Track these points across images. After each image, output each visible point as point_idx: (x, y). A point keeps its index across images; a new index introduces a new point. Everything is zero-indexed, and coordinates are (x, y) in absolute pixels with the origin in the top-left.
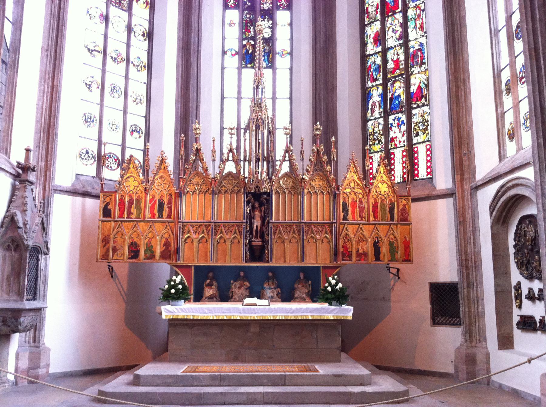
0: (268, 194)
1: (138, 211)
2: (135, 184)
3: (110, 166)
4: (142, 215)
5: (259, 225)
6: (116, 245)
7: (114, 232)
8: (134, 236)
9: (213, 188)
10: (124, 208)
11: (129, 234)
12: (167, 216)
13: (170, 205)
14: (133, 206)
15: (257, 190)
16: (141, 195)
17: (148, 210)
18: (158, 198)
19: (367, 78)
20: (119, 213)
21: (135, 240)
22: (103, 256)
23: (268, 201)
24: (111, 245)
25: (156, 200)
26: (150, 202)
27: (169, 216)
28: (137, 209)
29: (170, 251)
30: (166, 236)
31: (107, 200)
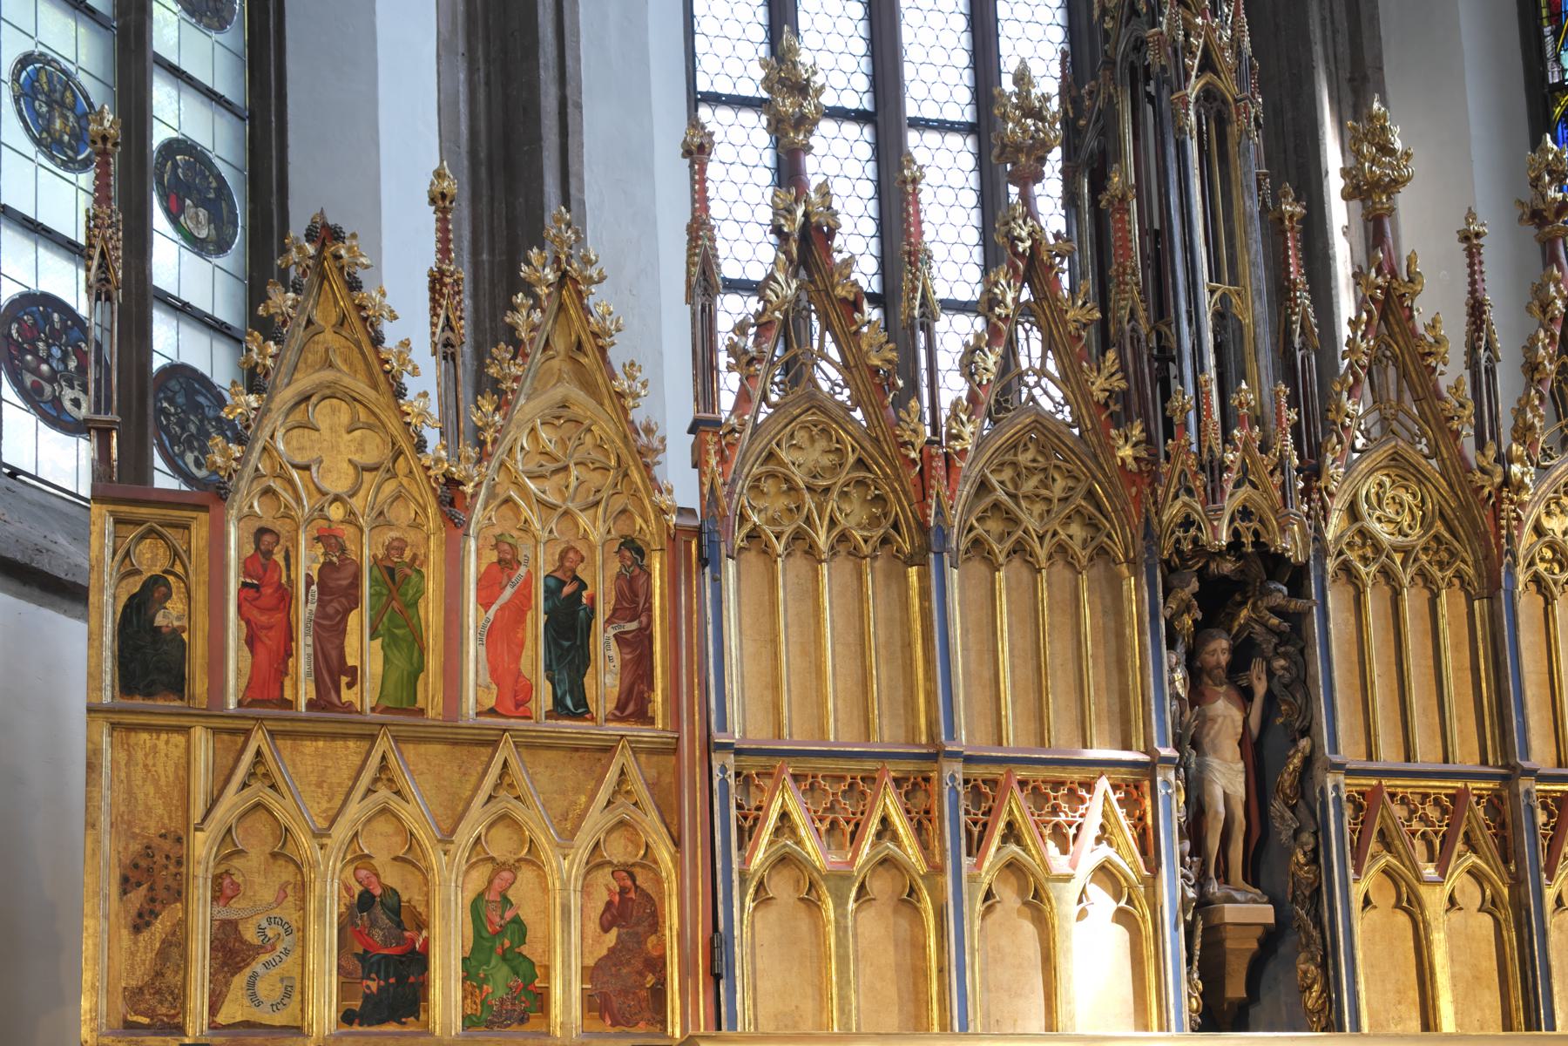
0: (1297, 578)
1: (400, 661)
2: (361, 448)
3: (48, 389)
4: (431, 690)
5: (1239, 790)
6: (231, 911)
7: (220, 812)
8: (381, 846)
9: (940, 512)
10: (289, 636)
11: (341, 832)
12: (621, 706)
13: (633, 626)
14: (359, 622)
15: (1248, 539)
16: (412, 536)
17: (473, 650)
18: (541, 564)
19: (1547, 30)
20: (247, 670)
21: (392, 877)
22: (134, 996)
23: (1297, 621)
24: (201, 915)
25: (528, 582)
26: (488, 588)
27: (633, 705)
28: (392, 643)
29: (658, 965)
30: (618, 851)
31: (151, 558)
